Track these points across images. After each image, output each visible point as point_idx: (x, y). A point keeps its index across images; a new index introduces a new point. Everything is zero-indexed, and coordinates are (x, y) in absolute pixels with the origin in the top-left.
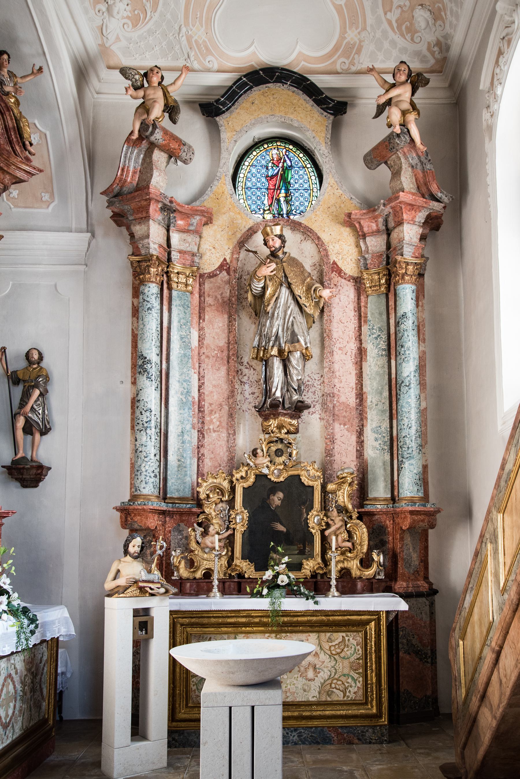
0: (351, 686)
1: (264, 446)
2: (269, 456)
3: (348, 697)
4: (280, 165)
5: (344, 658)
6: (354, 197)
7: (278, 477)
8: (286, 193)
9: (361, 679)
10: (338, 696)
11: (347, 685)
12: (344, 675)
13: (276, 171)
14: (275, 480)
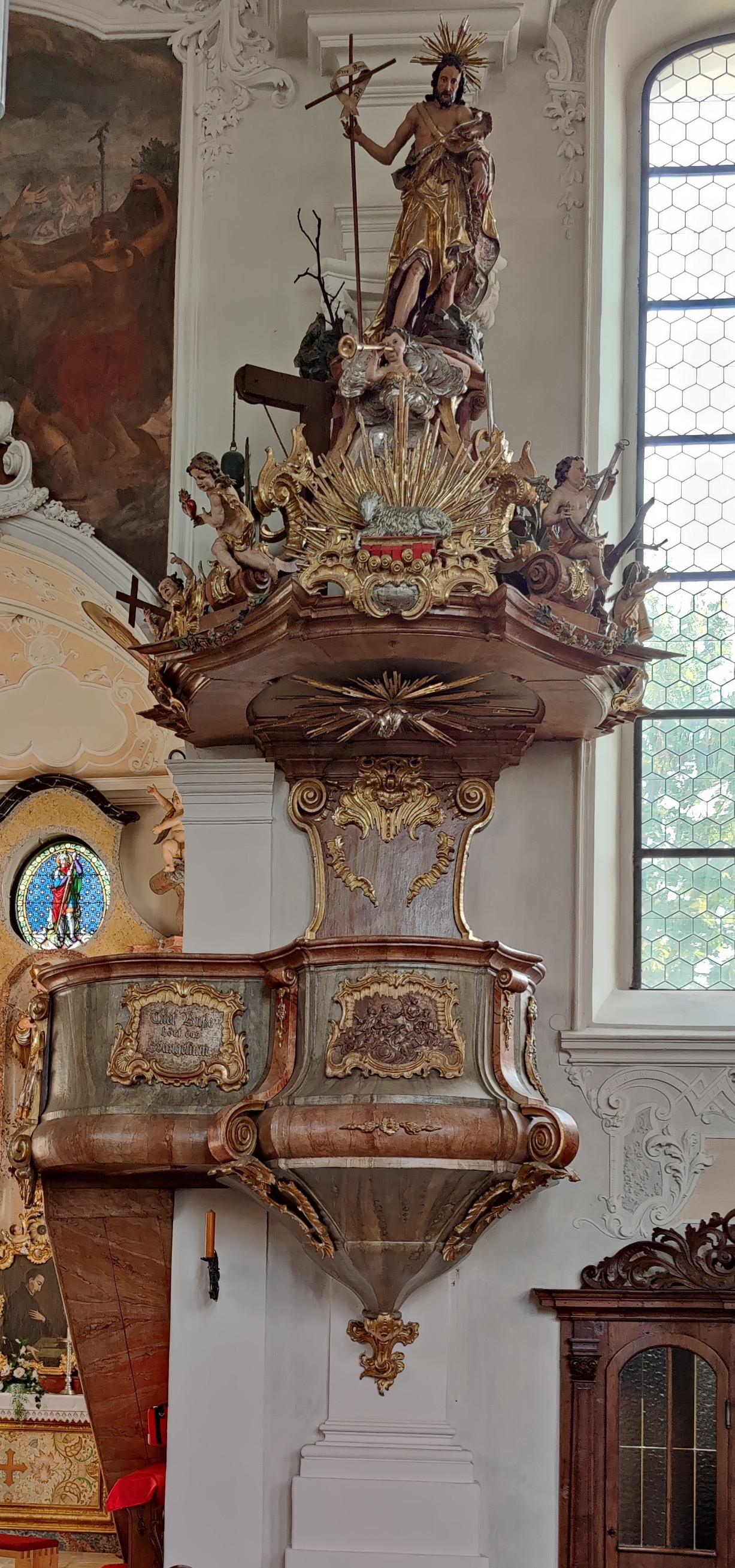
0: (86, 1491)
1: (24, 1223)
2: (30, 1233)
3: (83, 1502)
4: (69, 873)
5: (80, 1460)
6: (144, 922)
7: (40, 1258)
8: (74, 908)
9: (97, 1484)
10: (72, 1500)
11: (82, 1489)
12: (80, 1479)
13: (63, 881)
14: (36, 1261)
